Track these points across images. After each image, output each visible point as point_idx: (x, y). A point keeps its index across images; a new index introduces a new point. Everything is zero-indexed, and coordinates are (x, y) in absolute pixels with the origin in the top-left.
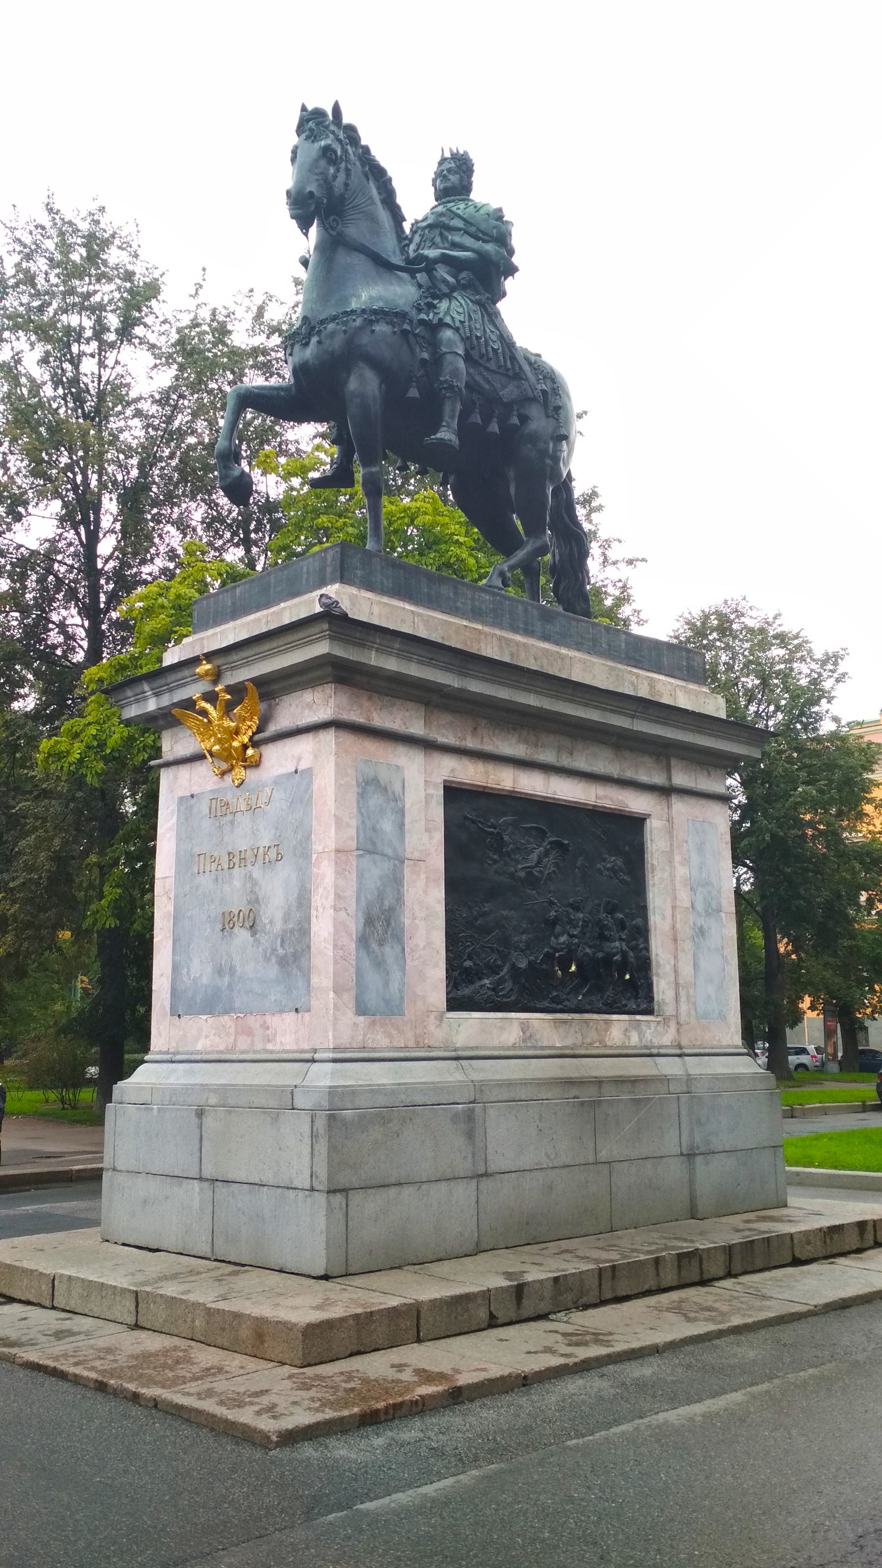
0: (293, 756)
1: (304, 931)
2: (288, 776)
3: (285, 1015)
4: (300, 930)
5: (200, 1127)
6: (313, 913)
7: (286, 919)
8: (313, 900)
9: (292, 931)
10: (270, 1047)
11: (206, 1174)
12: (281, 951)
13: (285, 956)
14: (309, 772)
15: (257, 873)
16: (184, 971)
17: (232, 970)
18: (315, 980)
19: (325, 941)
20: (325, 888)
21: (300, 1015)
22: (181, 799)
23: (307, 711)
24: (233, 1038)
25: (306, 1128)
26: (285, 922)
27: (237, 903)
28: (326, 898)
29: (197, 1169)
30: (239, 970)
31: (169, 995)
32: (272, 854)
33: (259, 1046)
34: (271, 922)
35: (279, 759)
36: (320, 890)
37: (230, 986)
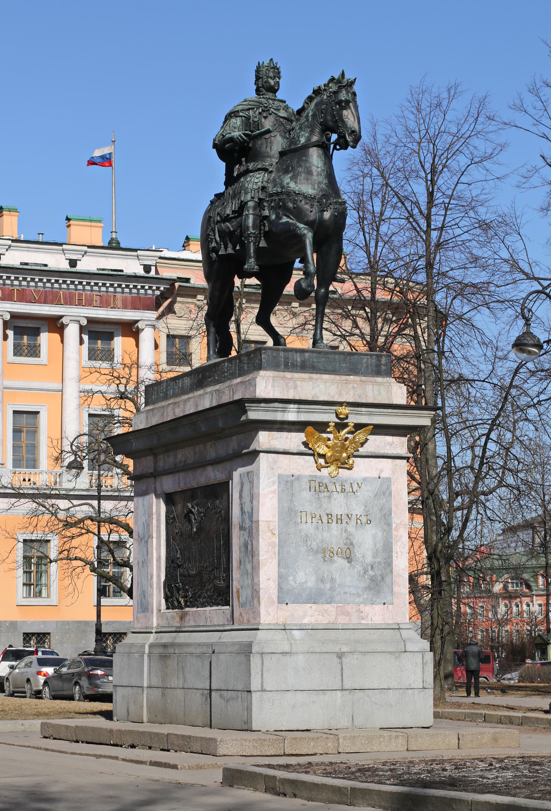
0: (377, 469)
1: (389, 564)
3: (374, 606)
4: (385, 563)
8: (394, 548)
9: (379, 563)
10: (363, 622)
11: (346, 687)
12: (371, 573)
14: (389, 479)
15: (351, 528)
16: (291, 578)
17: (333, 580)
18: (396, 589)
19: (403, 569)
20: (402, 543)
21: (386, 606)
22: (280, 476)
23: (388, 447)
24: (334, 617)
25: (420, 660)
26: (374, 557)
28: (403, 548)
29: (340, 685)
30: (338, 581)
31: (276, 592)
32: (364, 519)
33: (355, 620)
34: (363, 557)
35: (363, 468)
36: (399, 544)
37: (332, 589)
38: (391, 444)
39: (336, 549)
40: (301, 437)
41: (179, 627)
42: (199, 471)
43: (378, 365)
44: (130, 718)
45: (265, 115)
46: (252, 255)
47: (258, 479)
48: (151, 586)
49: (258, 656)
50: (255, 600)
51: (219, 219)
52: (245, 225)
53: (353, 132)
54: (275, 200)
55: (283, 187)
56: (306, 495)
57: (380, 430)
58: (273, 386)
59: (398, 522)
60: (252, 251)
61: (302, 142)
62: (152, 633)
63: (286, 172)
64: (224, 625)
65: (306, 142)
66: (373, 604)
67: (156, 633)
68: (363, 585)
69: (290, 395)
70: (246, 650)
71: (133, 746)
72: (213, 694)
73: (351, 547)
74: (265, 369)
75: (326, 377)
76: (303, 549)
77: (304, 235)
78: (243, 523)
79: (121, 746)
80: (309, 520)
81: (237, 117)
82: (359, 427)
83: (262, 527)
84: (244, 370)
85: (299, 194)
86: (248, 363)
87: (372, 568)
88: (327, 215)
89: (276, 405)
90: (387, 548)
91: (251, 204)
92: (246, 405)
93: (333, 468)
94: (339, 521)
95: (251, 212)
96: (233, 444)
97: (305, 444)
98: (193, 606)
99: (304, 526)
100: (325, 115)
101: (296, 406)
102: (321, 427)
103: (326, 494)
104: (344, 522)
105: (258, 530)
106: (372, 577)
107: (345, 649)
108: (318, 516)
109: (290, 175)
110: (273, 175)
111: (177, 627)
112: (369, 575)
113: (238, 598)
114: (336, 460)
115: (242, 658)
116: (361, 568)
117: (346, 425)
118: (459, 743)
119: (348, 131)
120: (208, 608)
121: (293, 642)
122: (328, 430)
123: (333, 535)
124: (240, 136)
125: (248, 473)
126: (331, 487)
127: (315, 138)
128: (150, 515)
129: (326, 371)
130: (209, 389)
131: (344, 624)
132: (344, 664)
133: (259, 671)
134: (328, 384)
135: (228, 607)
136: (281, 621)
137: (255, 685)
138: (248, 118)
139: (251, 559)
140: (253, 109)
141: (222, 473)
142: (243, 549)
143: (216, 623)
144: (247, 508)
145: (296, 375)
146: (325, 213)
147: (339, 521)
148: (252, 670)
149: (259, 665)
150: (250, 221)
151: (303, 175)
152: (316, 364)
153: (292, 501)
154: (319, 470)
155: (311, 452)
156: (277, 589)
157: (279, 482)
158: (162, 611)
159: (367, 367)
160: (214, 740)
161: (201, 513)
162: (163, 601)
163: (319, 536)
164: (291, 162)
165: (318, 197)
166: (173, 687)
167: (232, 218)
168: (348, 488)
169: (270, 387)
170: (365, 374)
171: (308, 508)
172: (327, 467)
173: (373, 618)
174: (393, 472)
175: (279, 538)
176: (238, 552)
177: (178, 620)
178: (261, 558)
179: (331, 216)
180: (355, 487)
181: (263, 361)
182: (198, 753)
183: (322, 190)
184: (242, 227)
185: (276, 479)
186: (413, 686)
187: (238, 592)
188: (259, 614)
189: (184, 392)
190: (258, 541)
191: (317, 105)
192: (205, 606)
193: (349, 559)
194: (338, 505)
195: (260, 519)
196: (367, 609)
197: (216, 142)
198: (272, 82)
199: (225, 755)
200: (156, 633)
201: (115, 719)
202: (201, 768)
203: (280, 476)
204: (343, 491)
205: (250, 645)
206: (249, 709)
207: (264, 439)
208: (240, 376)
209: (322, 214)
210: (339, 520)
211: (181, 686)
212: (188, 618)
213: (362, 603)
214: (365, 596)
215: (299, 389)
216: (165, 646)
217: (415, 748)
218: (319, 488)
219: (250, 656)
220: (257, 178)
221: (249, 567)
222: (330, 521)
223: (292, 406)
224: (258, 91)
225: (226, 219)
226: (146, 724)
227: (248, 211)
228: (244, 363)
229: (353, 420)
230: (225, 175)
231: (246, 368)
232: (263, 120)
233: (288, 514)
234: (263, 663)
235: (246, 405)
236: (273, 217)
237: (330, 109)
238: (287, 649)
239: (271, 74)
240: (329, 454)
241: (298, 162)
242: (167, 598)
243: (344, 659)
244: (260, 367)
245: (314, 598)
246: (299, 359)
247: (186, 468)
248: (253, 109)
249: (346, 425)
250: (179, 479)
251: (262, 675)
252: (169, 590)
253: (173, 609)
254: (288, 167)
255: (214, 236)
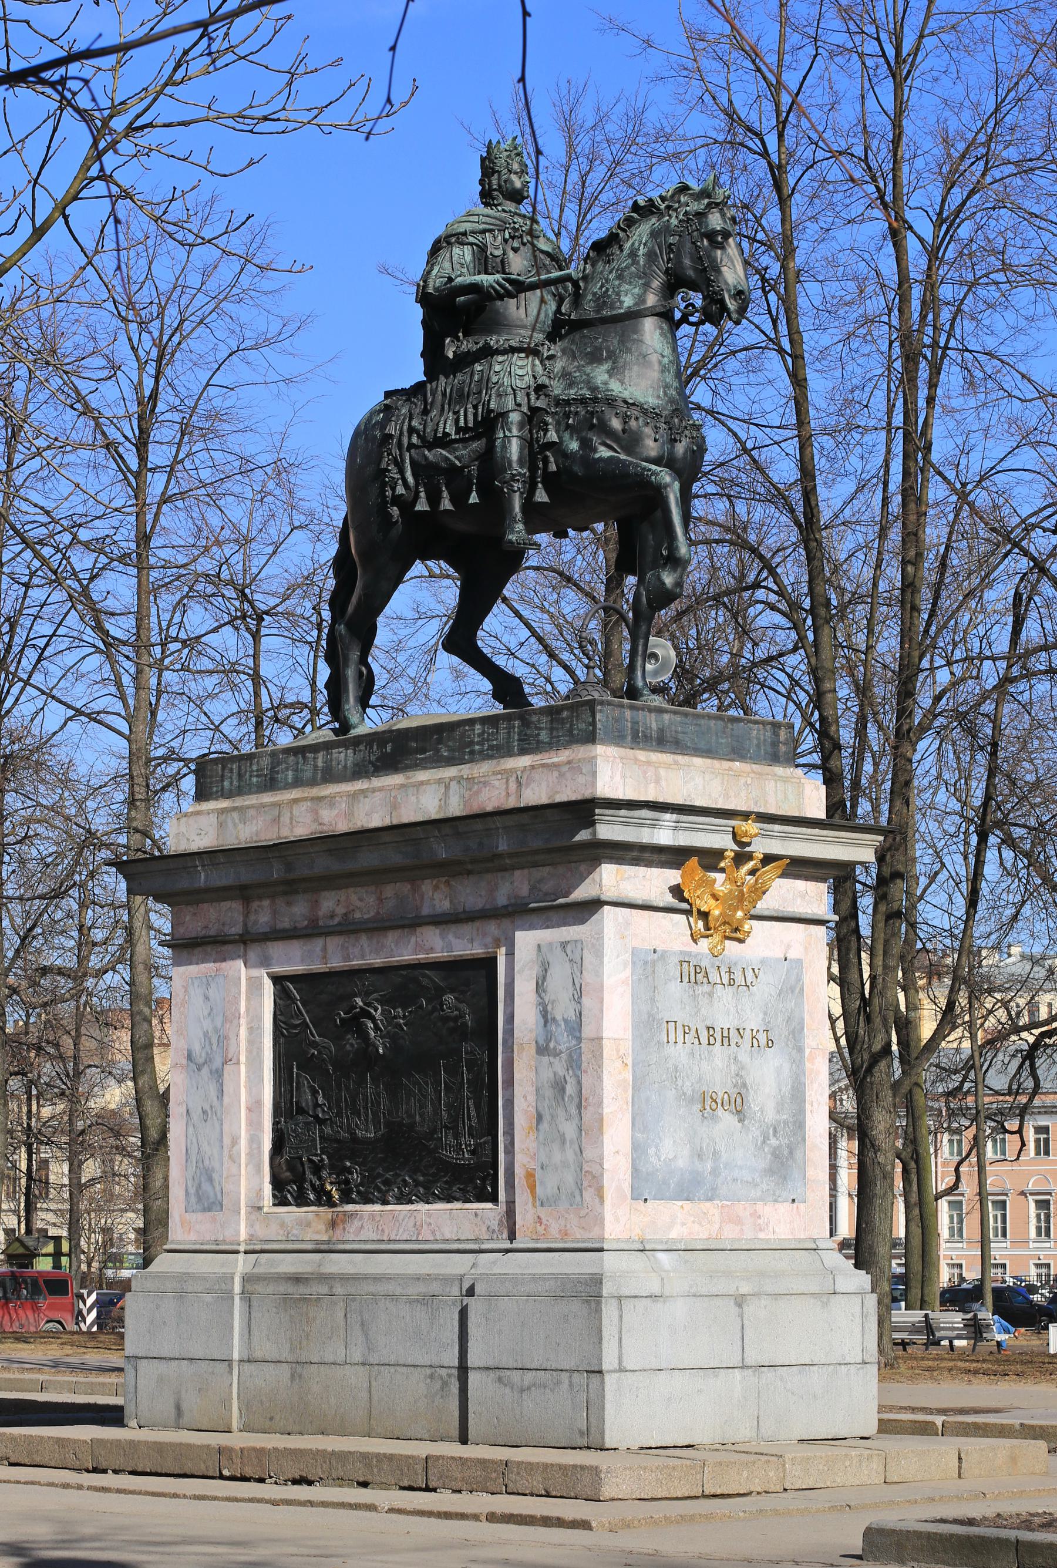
1: (799, 1125)
2: (778, 960)
3: (777, 1205)
5: (741, 1316)
6: (808, 1106)
7: (780, 1108)
9: (786, 1123)
10: (762, 1235)
11: (749, 1361)
12: (773, 1142)
13: (779, 1147)
14: (799, 962)
15: (744, 1056)
16: (652, 1151)
17: (716, 1154)
22: (635, 952)
24: (717, 1226)
25: (857, 1309)
27: (720, 1084)
29: (740, 1358)
32: (762, 1038)
33: (749, 1234)
34: (762, 1110)
36: (815, 1086)
37: (715, 1172)
38: (803, 895)
39: (720, 1095)
40: (673, 876)
41: (328, 1242)
42: (391, 937)
43: (775, 744)
44: (185, 1420)
45: (516, 244)
46: (519, 516)
47: (599, 954)
48: (234, 1159)
49: (614, 1302)
50: (588, 1194)
51: (415, 440)
52: (503, 458)
53: (740, 293)
54: (577, 413)
55: (594, 389)
56: (675, 989)
57: (800, 868)
58: (624, 777)
59: (814, 1044)
60: (517, 508)
61: (626, 305)
62: (238, 1252)
63: (595, 358)
64: (477, 1240)
65: (636, 304)
66: (776, 1201)
67: (246, 1252)
68: (762, 1164)
69: (650, 794)
70: (590, 1293)
71: (364, 1484)
72: (473, 1377)
73: (743, 1091)
74: (603, 742)
75: (698, 761)
76: (671, 1094)
77: (666, 486)
78: (548, 1041)
79: (262, 1480)
80: (680, 1039)
81: (463, 244)
82: (768, 859)
83: (608, 1050)
84: (538, 742)
85: (633, 404)
86: (552, 729)
87: (775, 1131)
88: (680, 448)
89: (645, 813)
90: (798, 1095)
91: (515, 417)
92: (597, 811)
93: (717, 938)
94: (726, 1040)
95: (515, 432)
96: (516, 885)
97: (677, 891)
98: (367, 1200)
99: (671, 1050)
100: (679, 256)
101: (674, 817)
102: (710, 859)
103: (706, 988)
104: (733, 1043)
105: (598, 1056)
106: (775, 1149)
107: (744, 1290)
108: (693, 1031)
109: (605, 367)
110: (559, 365)
111: (317, 1242)
112: (770, 1145)
113: (532, 1188)
114: (725, 923)
115: (576, 1307)
116: (758, 1133)
117: (749, 857)
118: (960, 1467)
119: (729, 291)
120: (422, 1207)
121: (664, 1274)
122: (722, 865)
123: (715, 1069)
124: (498, 283)
125: (564, 945)
126: (714, 976)
127: (651, 300)
128: (231, 1018)
129: (707, 752)
130: (422, 775)
131: (733, 1240)
132: (745, 1317)
133: (615, 1331)
134: (707, 777)
135: (490, 1205)
136: (636, 1234)
137: (609, 1362)
138: (482, 249)
139: (573, 1111)
140: (490, 231)
141: (472, 941)
142: (548, 1093)
143: (448, 1236)
144: (564, 1009)
145: (656, 757)
146: (678, 444)
147: (726, 1040)
148: (604, 1329)
149: (616, 1320)
150: (514, 449)
151: (635, 368)
152: (680, 736)
153: (653, 1000)
154: (695, 941)
155: (685, 906)
156: (629, 1172)
157: (634, 963)
158: (265, 1210)
159: (758, 746)
160: (595, 1471)
161: (395, 1017)
162: (268, 1189)
163: (696, 1068)
164: (604, 340)
165: (665, 413)
166: (329, 1358)
167: (456, 441)
168: (738, 977)
169: (618, 778)
170: (755, 759)
171: (681, 1016)
172: (707, 937)
173: (777, 1230)
174: (806, 948)
175: (634, 1071)
176: (532, 1098)
177: (322, 1227)
178: (606, 1111)
179: (685, 453)
180: (750, 974)
181: (599, 725)
182: (532, 1495)
183: (672, 401)
184: (490, 462)
185: (628, 956)
186: (848, 1360)
187: (530, 1176)
188: (600, 1220)
189: (329, 776)
190: (600, 1078)
191: (654, 234)
192: (411, 1202)
193: (740, 1114)
194: (724, 1009)
195: (606, 1034)
196: (767, 1210)
197: (430, 290)
198: (518, 184)
199: (612, 1499)
200: (246, 1252)
201: (133, 1423)
202: (629, 1526)
203: (635, 952)
204: (732, 982)
205: (597, 1281)
206: (595, 1407)
207: (611, 879)
208: (523, 752)
209: (673, 447)
210: (726, 1039)
211: (358, 1358)
212: (357, 1223)
213: (761, 1199)
214: (765, 1187)
215: (663, 783)
216: (297, 1279)
217: (896, 1479)
218: (694, 974)
219: (599, 1303)
220: (520, 367)
221: (569, 1129)
222: (712, 1041)
223: (668, 816)
224: (487, 197)
225: (443, 441)
226: (236, 1434)
227: (510, 431)
228: (540, 729)
229: (760, 847)
230: (422, 355)
231: (544, 736)
232: (511, 254)
233: (649, 1026)
234: (621, 1316)
235: (597, 811)
236: (574, 446)
237: (689, 245)
238: (656, 1290)
239: (516, 167)
240: (717, 912)
241: (622, 342)
242: (278, 1184)
243: (745, 1308)
244: (591, 738)
245: (688, 1189)
246: (654, 726)
247: (349, 928)
248: (490, 231)
249: (749, 857)
250: (324, 949)
251: (620, 1339)
252: (291, 1167)
253: (298, 1205)
254: (599, 349)
255: (402, 471)
